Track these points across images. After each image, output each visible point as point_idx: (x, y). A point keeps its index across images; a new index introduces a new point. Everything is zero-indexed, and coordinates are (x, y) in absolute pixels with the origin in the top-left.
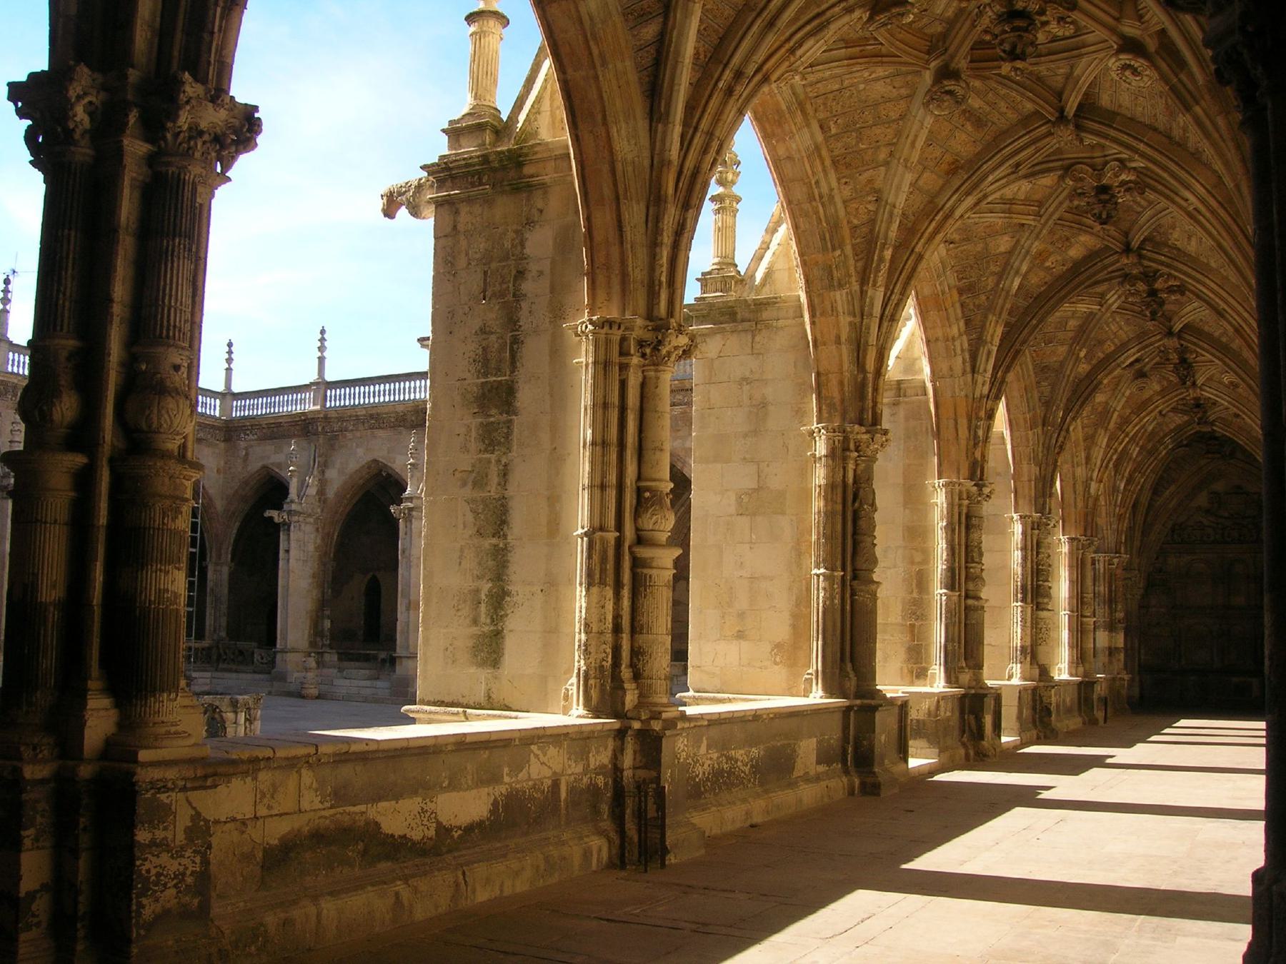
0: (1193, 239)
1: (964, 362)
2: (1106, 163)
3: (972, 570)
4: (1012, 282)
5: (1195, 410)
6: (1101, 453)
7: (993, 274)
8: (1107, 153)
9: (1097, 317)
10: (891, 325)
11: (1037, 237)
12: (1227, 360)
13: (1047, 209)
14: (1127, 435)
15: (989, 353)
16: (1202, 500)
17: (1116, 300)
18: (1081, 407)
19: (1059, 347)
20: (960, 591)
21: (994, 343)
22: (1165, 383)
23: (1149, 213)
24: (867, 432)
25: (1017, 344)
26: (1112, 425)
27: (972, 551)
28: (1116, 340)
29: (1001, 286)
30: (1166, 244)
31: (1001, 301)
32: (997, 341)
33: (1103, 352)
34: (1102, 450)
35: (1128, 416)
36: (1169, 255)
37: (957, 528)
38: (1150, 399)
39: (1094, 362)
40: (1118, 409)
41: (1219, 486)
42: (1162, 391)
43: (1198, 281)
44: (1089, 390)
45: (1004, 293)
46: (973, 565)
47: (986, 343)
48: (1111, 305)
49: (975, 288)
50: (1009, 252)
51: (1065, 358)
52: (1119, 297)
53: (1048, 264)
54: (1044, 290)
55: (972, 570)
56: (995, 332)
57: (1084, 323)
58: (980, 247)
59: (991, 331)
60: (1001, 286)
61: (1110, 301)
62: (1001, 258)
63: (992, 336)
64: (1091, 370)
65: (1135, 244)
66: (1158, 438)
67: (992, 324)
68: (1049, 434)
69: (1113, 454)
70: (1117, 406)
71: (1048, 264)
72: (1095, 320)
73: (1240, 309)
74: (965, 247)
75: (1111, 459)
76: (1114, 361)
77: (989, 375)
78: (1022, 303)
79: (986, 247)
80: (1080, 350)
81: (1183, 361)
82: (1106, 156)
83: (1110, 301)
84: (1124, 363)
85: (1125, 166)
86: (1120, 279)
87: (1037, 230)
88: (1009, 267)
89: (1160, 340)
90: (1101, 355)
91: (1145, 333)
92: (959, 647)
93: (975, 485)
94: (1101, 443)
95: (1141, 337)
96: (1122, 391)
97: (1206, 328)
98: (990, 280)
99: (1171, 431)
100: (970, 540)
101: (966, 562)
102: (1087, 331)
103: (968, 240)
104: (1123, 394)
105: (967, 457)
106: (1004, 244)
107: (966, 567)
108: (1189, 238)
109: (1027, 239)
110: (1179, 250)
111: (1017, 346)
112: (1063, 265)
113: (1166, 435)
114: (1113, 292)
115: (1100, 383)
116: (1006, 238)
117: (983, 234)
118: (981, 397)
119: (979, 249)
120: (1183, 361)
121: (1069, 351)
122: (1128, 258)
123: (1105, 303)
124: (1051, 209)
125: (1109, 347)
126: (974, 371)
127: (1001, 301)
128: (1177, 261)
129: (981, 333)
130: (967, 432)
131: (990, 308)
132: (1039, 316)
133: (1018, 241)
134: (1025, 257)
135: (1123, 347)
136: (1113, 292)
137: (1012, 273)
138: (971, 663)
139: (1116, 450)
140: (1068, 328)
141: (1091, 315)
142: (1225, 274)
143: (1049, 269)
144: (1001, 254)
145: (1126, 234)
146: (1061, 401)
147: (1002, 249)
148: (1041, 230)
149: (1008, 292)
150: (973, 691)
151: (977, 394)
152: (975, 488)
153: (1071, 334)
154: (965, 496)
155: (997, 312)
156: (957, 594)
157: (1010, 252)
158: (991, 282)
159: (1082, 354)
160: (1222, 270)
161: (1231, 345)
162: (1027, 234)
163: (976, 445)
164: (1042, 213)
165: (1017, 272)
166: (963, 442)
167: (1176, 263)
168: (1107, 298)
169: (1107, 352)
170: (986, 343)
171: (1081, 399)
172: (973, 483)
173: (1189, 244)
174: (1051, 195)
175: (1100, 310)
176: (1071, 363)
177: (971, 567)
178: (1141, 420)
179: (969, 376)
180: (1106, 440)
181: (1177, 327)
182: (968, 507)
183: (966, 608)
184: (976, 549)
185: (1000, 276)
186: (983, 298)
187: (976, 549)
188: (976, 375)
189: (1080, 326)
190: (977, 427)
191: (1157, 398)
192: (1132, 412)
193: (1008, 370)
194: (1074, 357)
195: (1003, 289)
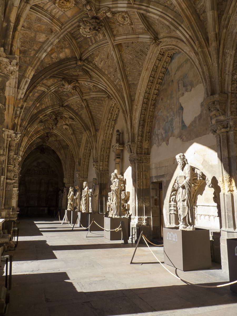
0: (103, 62)
1: (16, 83)
2: (99, 9)
3: (10, 168)
4: (42, 55)
5: (46, 137)
6: (25, 143)
7: (34, 50)
8: (101, 5)
9: (46, 94)
10: (26, 5)
11: (58, 38)
12: (77, 117)
13: (65, 27)
14: (32, 140)
15: (27, 82)
16: (35, 164)
17: (54, 89)
18: (32, 123)
19: (30, 102)
20: (4, 176)
21: (29, 78)
22: (44, 127)
23: (95, 46)
24: (7, 58)
25: (36, 83)
26: (29, 136)
27: (10, 160)
28: (46, 105)
29: (37, 56)
30: (92, 63)
31: (35, 62)
32: (31, 77)
33: (41, 108)
34: (25, 143)
35: (33, 135)
36: (92, 66)
37: (6, 149)
38: (40, 131)
39: (38, 110)
40: (32, 131)
41: (40, 161)
42: (43, 129)
43: (100, 77)
44: (35, 119)
45: (37, 59)
46: (10, 166)
47: (26, 77)
48: (51, 91)
49: (26, 53)
50: (43, 43)
51: (31, 106)
52: (55, 88)
53: (52, 56)
54: (48, 66)
55: (10, 168)
56: (30, 73)
57: (40, 95)
58: (33, 35)
59: (29, 73)
60: (37, 56)
61: (51, 89)
62: (39, 44)
63: (29, 75)
64: (37, 112)
65: (84, 58)
66: (32, 145)
67: (30, 70)
68: (22, 130)
69: (28, 145)
70: (32, 130)
71: (52, 56)
72: (45, 95)
73: (113, 89)
74: (28, 32)
75: (27, 146)
76: (44, 111)
77: (25, 90)
78: (40, 69)
79: (35, 37)
80: (37, 104)
81: (56, 119)
82: (100, 6)
83: (51, 89)
84: (47, 112)
85: (110, 10)
86: (61, 79)
87: (58, 35)
88: (42, 49)
89: (58, 108)
90: (40, 109)
91: (54, 105)
92: (2, 200)
93: (14, 133)
94: (26, 141)
95: (53, 106)
96: (34, 126)
97: (72, 107)
98: (32, 52)
99: (36, 143)
100: (9, 156)
101: (8, 164)
102: (41, 98)
103: (29, 28)
104: (35, 127)
105: (12, 121)
106: (42, 38)
107: (7, 166)
108: (101, 62)
109: (53, 38)
110: (96, 65)
111: (35, 84)
112: (56, 59)
113: (34, 144)
114: (53, 86)
115: (39, 117)
116: (44, 35)
117: (36, 29)
118: (20, 99)
119: (32, 36)
120: (56, 119)
121: (33, 104)
122: (81, 62)
123: (50, 89)
124: (67, 27)
125: (43, 107)
126: (18, 88)
127: (35, 62)
128: (95, 69)
129: (24, 73)
130: (13, 111)
131: (30, 64)
132: (45, 75)
133: (48, 39)
134: (51, 45)
135: (47, 108)
136: (53, 86)
137: (43, 51)
138: (7, 207)
139: (29, 143)
140: (34, 96)
141: (44, 92)
142: (109, 77)
143: (52, 58)
144: (40, 42)
145: (81, 54)
146: (27, 120)
147: (41, 40)
148: (60, 35)
149: (39, 59)
150: (8, 220)
151: (19, 98)
152: (14, 134)
153: (35, 98)
154: (9, 137)
155: (33, 65)
156: (4, 177)
157: (44, 43)
158: (33, 53)
159: (38, 105)
160: (109, 75)
161: (78, 113)
162: (53, 36)
163: (15, 118)
164: (62, 28)
165: (45, 51)
166: (11, 115)
167: (94, 70)
168: (51, 88)
169: (42, 108)
170: (26, 77)
171: (33, 121)
172: (14, 132)
173: (100, 64)
174: (69, 21)
175: (47, 91)
176: (33, 108)
177: (9, 167)
178: (36, 136)
179: (16, 89)
180: (27, 140)
181: (65, 104)
182: (10, 142)
183: (7, 183)
184: (12, 159)
185: (37, 52)
186: (28, 59)
187: (12, 159)
188: (19, 90)
189: (39, 96)
190: (17, 110)
191: (41, 131)
192: (34, 134)
193: (30, 92)
194: (35, 106)
195: (37, 57)
